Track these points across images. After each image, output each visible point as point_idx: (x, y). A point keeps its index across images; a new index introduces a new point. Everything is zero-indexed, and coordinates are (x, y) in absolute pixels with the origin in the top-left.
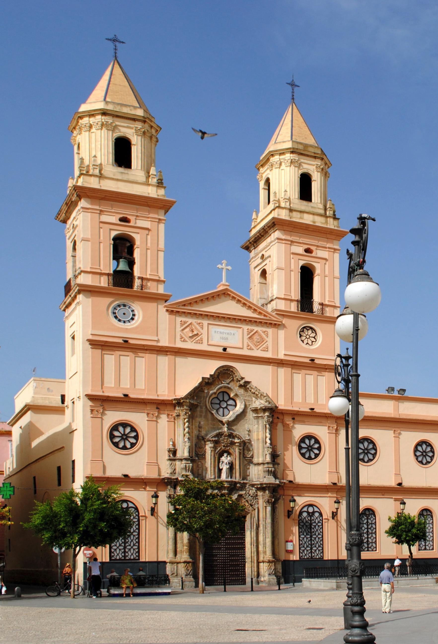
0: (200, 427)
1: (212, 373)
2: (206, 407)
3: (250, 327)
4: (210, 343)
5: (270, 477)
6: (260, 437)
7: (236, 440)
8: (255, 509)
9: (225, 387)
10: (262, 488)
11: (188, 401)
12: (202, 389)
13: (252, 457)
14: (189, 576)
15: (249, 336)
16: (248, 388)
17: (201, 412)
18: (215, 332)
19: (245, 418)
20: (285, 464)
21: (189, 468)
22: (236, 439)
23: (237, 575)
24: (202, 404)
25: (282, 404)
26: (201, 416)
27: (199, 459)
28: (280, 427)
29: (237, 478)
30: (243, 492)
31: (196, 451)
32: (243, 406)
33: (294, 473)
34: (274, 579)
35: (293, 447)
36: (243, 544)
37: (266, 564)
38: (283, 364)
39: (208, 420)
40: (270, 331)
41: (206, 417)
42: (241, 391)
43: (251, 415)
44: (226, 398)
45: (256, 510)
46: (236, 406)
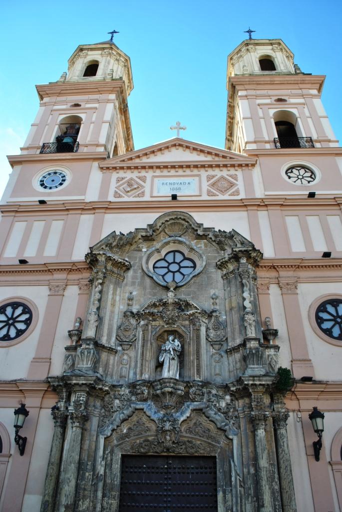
1: (151, 223)
11: (101, 252)
15: (210, 182)
16: (211, 238)
18: (163, 184)
24: (136, 268)
26: (133, 283)
31: (117, 335)
39: (145, 288)
46: (194, 267)
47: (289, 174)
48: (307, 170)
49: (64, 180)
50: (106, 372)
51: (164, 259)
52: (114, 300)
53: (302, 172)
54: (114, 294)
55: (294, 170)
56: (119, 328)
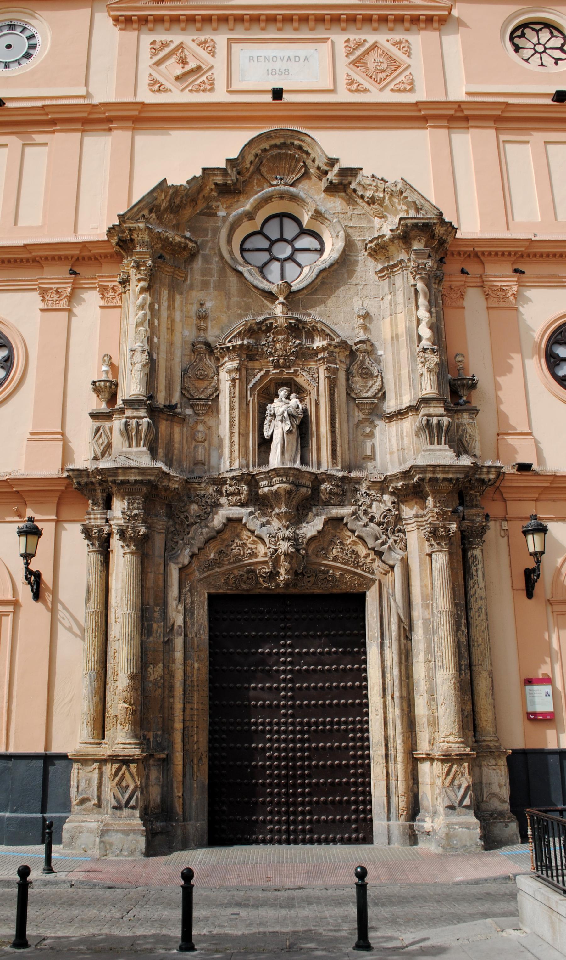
0: (202, 317)
1: (234, 155)
2: (222, 257)
3: (354, 36)
4: (234, 87)
5: (436, 447)
6: (402, 329)
7: (319, 343)
8: (392, 567)
9: (282, 196)
10: (413, 487)
11: (141, 225)
12: (209, 207)
13: (381, 395)
14: (126, 812)
15: (352, 58)
16: (355, 191)
17: (206, 272)
18: (251, 58)
19: (353, 281)
20: (501, 417)
21: (138, 432)
22: (317, 339)
23: (342, 807)
24: (207, 251)
25: (471, 226)
26: (205, 285)
27: (197, 414)
28: (474, 299)
29: (323, 462)
30: (345, 511)
32: (340, 244)
33: (537, 443)
34: (469, 825)
35: (528, 362)
36: (361, 691)
37: (438, 768)
38: (467, 119)
39: (228, 296)
40: (418, 40)
41: (221, 286)
42: (334, 205)
43: (367, 267)
44: (291, 230)
45: (398, 570)
46: (321, 251)
47: (517, 41)
48: (556, 33)
49: (33, 47)
50: (170, 456)
51: (260, 233)
52: (171, 320)
53: (545, 35)
54: (171, 307)
55: (528, 31)
56: (185, 372)
